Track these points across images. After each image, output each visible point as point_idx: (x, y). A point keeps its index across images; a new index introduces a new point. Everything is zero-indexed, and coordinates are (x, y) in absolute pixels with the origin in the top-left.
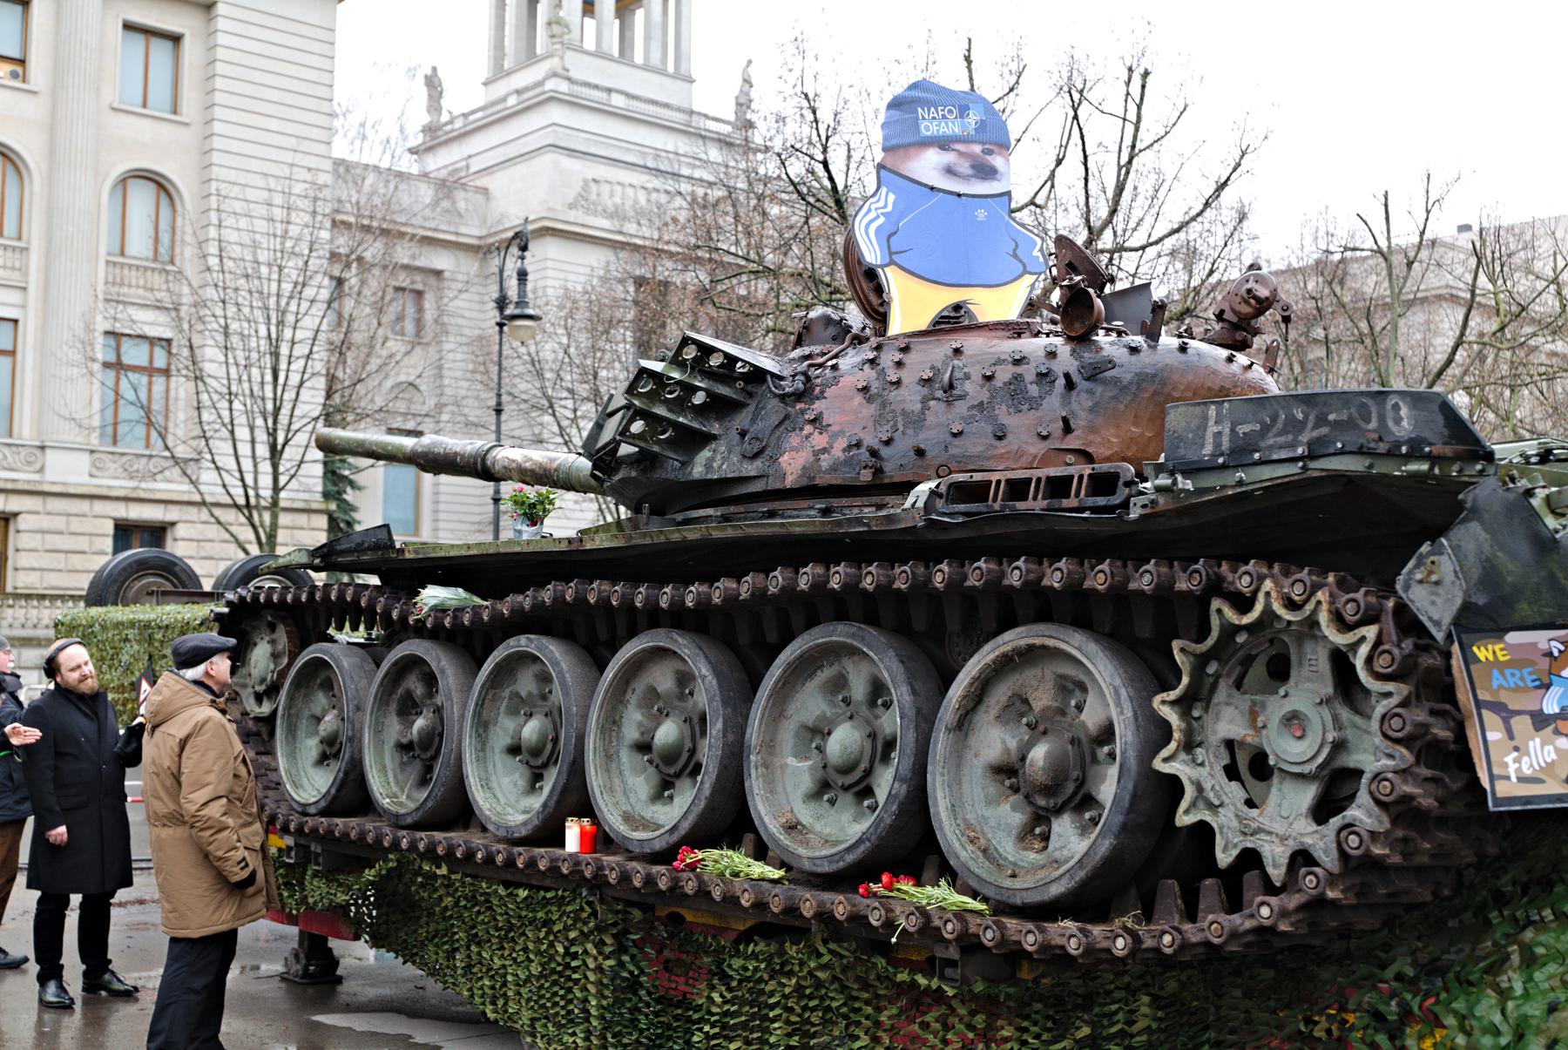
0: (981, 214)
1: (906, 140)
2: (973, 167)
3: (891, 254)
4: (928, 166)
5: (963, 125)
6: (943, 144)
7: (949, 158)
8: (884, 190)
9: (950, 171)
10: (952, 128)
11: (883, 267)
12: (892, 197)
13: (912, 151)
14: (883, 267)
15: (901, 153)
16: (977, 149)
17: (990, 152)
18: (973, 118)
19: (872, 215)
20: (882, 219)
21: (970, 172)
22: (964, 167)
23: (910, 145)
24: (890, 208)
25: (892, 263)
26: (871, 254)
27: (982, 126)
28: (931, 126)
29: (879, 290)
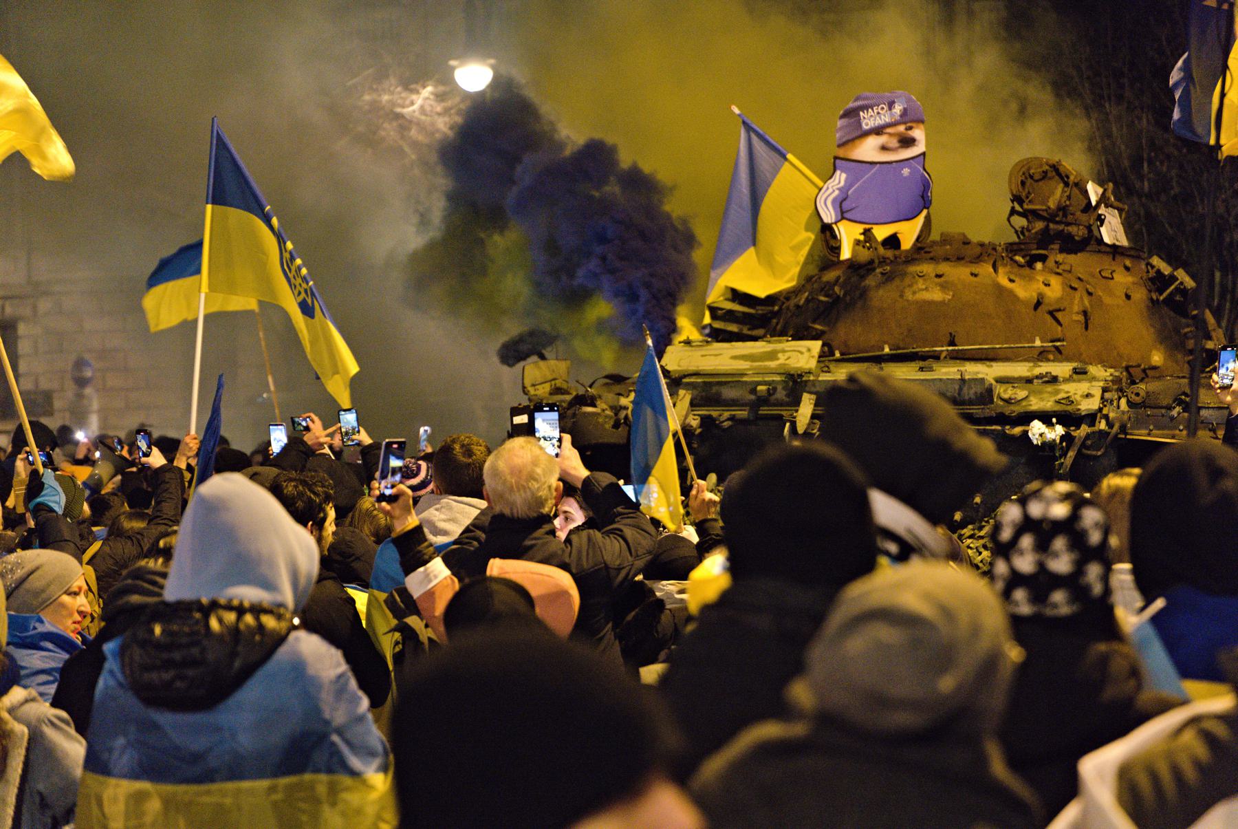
0: (906, 172)
1: (850, 137)
2: (900, 141)
3: (842, 213)
4: (868, 150)
5: (892, 115)
6: (878, 131)
7: (882, 140)
8: (838, 172)
9: (884, 148)
10: (885, 118)
11: (836, 223)
12: (844, 176)
13: (857, 142)
14: (836, 223)
15: (850, 145)
16: (901, 128)
17: (910, 128)
18: (898, 109)
19: (830, 190)
20: (837, 192)
21: (897, 145)
22: (894, 143)
23: (853, 140)
24: (842, 183)
25: (843, 218)
26: (828, 216)
27: (905, 113)
28: (869, 120)
29: (834, 236)
